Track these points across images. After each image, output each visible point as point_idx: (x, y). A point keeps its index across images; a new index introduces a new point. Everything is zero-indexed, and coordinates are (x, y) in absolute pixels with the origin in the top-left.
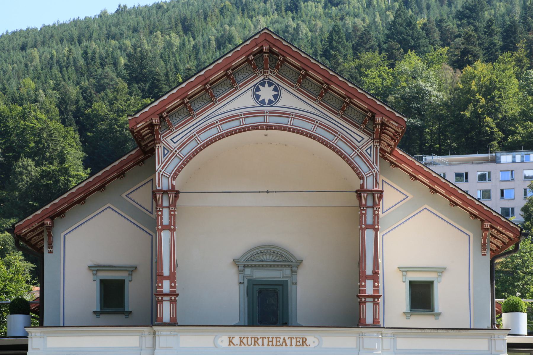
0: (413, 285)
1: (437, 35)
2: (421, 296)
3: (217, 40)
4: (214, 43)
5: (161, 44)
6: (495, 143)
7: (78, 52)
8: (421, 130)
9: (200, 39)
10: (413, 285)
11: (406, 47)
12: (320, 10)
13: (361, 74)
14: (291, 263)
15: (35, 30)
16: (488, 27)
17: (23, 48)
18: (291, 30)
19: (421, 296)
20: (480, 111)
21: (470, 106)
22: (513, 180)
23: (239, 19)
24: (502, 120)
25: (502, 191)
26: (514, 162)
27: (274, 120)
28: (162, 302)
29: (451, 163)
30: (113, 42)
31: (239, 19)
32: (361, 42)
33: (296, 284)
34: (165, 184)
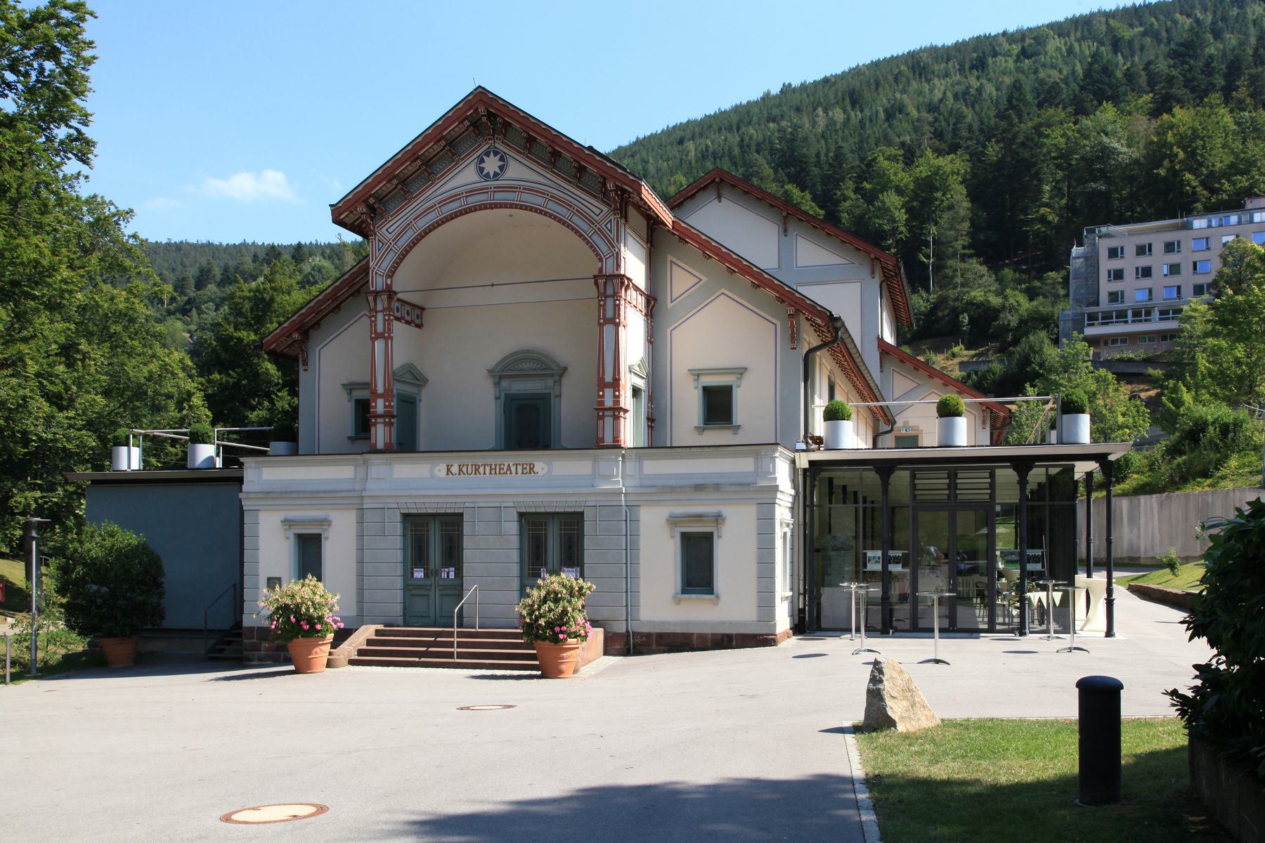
0: (707, 390)
1: (1143, 80)
2: (718, 405)
3: (886, 111)
4: (882, 115)
5: (822, 121)
6: (1199, 205)
7: (734, 139)
8: (1106, 196)
9: (867, 112)
10: (707, 390)
11: (1101, 97)
12: (1011, 64)
13: (1041, 135)
15: (695, 121)
16: (1207, 65)
17: (681, 142)
18: (972, 91)
19: (718, 405)
20: (1177, 167)
21: (1166, 163)
22: (1208, 249)
23: (915, 85)
24: (1207, 176)
25: (1195, 264)
26: (1210, 226)
28: (375, 424)
29: (1131, 233)
30: (771, 125)
31: (915, 85)
32: (1048, 96)
33: (560, 396)
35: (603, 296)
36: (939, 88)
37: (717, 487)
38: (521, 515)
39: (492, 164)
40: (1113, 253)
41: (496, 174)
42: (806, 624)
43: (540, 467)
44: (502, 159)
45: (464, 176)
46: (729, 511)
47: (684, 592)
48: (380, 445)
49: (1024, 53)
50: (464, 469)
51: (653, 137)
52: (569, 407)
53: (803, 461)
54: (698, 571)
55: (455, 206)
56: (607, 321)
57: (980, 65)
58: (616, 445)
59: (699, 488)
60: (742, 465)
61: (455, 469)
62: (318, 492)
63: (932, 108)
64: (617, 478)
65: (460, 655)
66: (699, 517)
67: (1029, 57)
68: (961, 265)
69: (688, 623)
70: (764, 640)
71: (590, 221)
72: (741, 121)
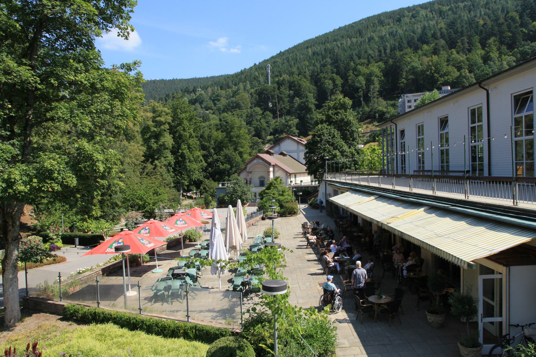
3: (368, 39)
4: (367, 40)
5: (349, 42)
7: (323, 47)
17: (307, 48)
18: (394, 32)
23: (379, 28)
31: (379, 28)
36: (384, 31)
40: (409, 101)
49: (413, 16)
51: (299, 45)
57: (399, 20)
63: (382, 38)
67: (414, 17)
68: (376, 100)
72: (325, 41)
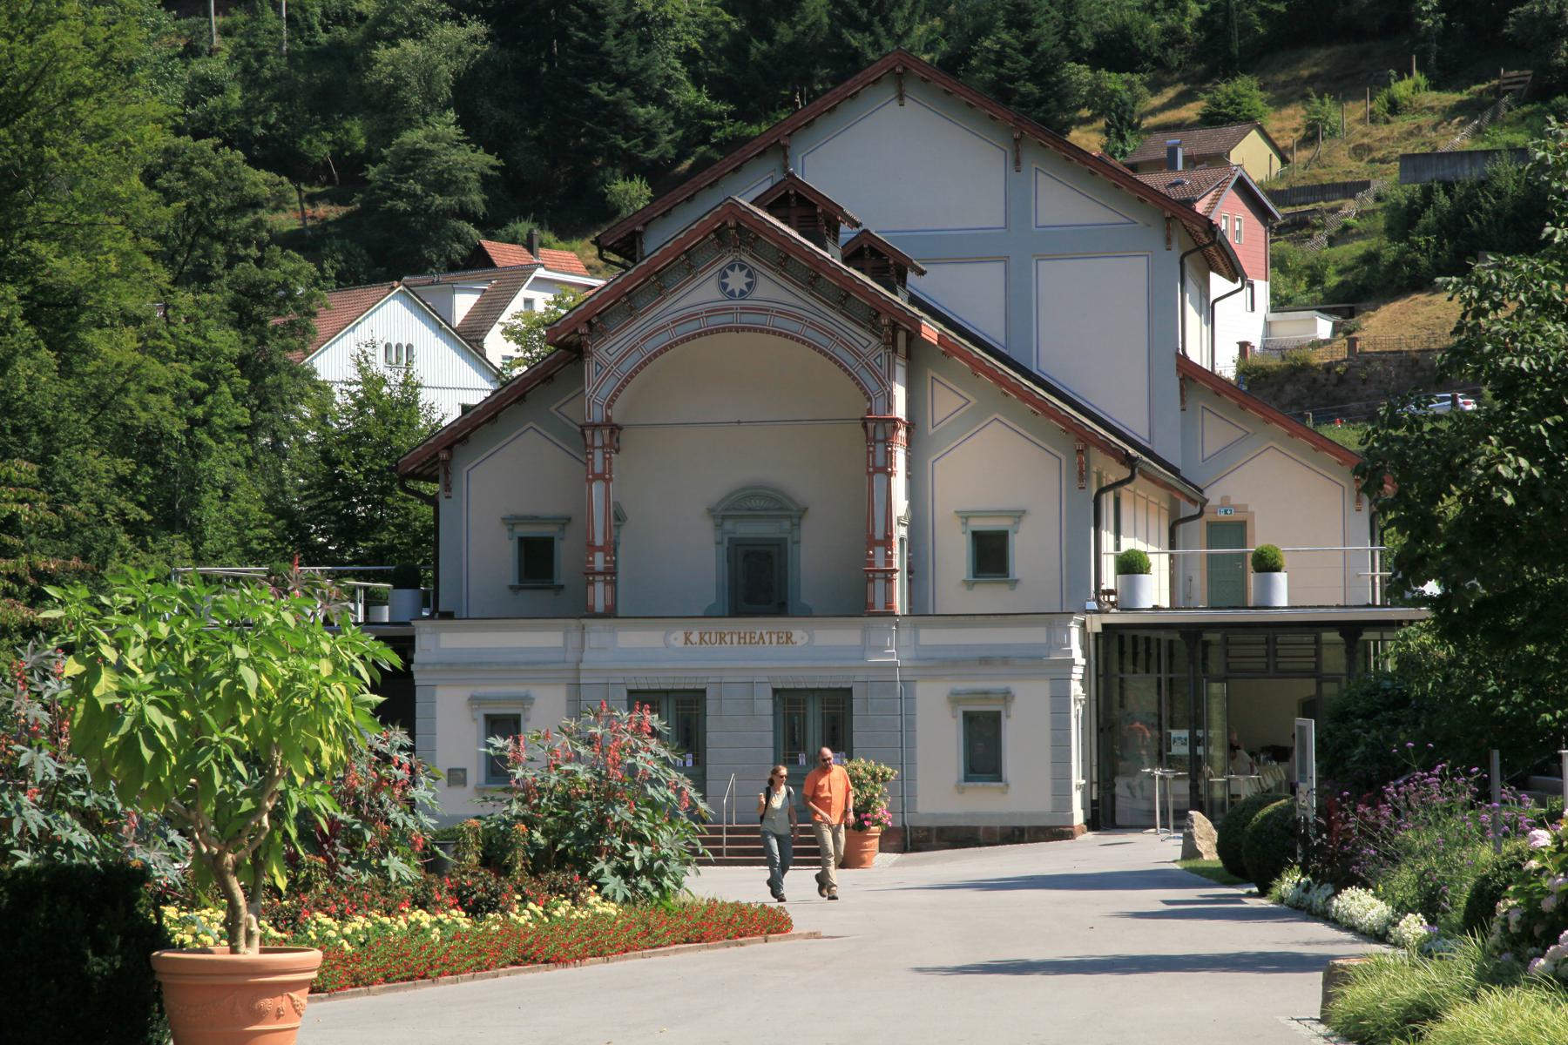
0: (977, 536)
2: (990, 555)
10: (977, 536)
14: (794, 513)
19: (990, 555)
27: (747, 319)
33: (798, 542)
34: (597, 415)
35: (871, 440)
37: (1005, 660)
38: (775, 691)
39: (737, 280)
41: (742, 293)
42: (1102, 818)
43: (799, 636)
44: (749, 275)
45: (702, 292)
46: (1017, 687)
47: (967, 779)
48: (599, 606)
50: (707, 637)
52: (813, 557)
53: (1095, 624)
54: (983, 753)
55: (693, 327)
56: (878, 470)
58: (889, 613)
59: (985, 661)
60: (1034, 635)
61: (695, 637)
62: (516, 663)
64: (892, 649)
65: (730, 853)
66: (986, 694)
69: (974, 815)
70: (1061, 833)
71: (858, 355)
